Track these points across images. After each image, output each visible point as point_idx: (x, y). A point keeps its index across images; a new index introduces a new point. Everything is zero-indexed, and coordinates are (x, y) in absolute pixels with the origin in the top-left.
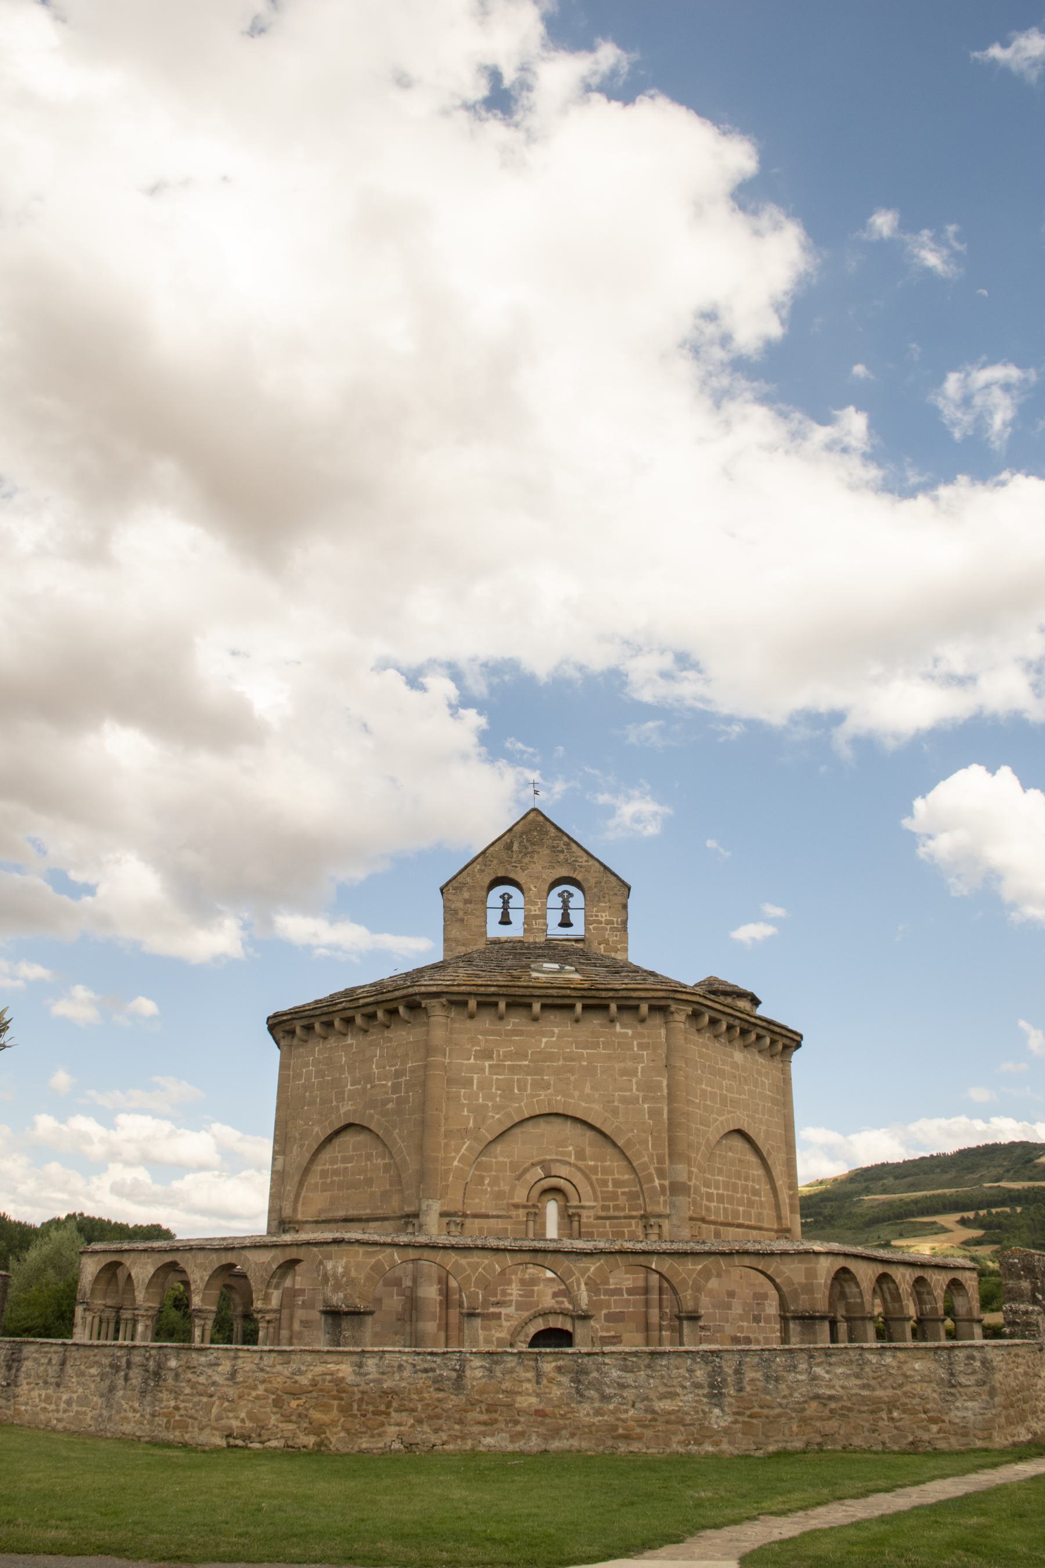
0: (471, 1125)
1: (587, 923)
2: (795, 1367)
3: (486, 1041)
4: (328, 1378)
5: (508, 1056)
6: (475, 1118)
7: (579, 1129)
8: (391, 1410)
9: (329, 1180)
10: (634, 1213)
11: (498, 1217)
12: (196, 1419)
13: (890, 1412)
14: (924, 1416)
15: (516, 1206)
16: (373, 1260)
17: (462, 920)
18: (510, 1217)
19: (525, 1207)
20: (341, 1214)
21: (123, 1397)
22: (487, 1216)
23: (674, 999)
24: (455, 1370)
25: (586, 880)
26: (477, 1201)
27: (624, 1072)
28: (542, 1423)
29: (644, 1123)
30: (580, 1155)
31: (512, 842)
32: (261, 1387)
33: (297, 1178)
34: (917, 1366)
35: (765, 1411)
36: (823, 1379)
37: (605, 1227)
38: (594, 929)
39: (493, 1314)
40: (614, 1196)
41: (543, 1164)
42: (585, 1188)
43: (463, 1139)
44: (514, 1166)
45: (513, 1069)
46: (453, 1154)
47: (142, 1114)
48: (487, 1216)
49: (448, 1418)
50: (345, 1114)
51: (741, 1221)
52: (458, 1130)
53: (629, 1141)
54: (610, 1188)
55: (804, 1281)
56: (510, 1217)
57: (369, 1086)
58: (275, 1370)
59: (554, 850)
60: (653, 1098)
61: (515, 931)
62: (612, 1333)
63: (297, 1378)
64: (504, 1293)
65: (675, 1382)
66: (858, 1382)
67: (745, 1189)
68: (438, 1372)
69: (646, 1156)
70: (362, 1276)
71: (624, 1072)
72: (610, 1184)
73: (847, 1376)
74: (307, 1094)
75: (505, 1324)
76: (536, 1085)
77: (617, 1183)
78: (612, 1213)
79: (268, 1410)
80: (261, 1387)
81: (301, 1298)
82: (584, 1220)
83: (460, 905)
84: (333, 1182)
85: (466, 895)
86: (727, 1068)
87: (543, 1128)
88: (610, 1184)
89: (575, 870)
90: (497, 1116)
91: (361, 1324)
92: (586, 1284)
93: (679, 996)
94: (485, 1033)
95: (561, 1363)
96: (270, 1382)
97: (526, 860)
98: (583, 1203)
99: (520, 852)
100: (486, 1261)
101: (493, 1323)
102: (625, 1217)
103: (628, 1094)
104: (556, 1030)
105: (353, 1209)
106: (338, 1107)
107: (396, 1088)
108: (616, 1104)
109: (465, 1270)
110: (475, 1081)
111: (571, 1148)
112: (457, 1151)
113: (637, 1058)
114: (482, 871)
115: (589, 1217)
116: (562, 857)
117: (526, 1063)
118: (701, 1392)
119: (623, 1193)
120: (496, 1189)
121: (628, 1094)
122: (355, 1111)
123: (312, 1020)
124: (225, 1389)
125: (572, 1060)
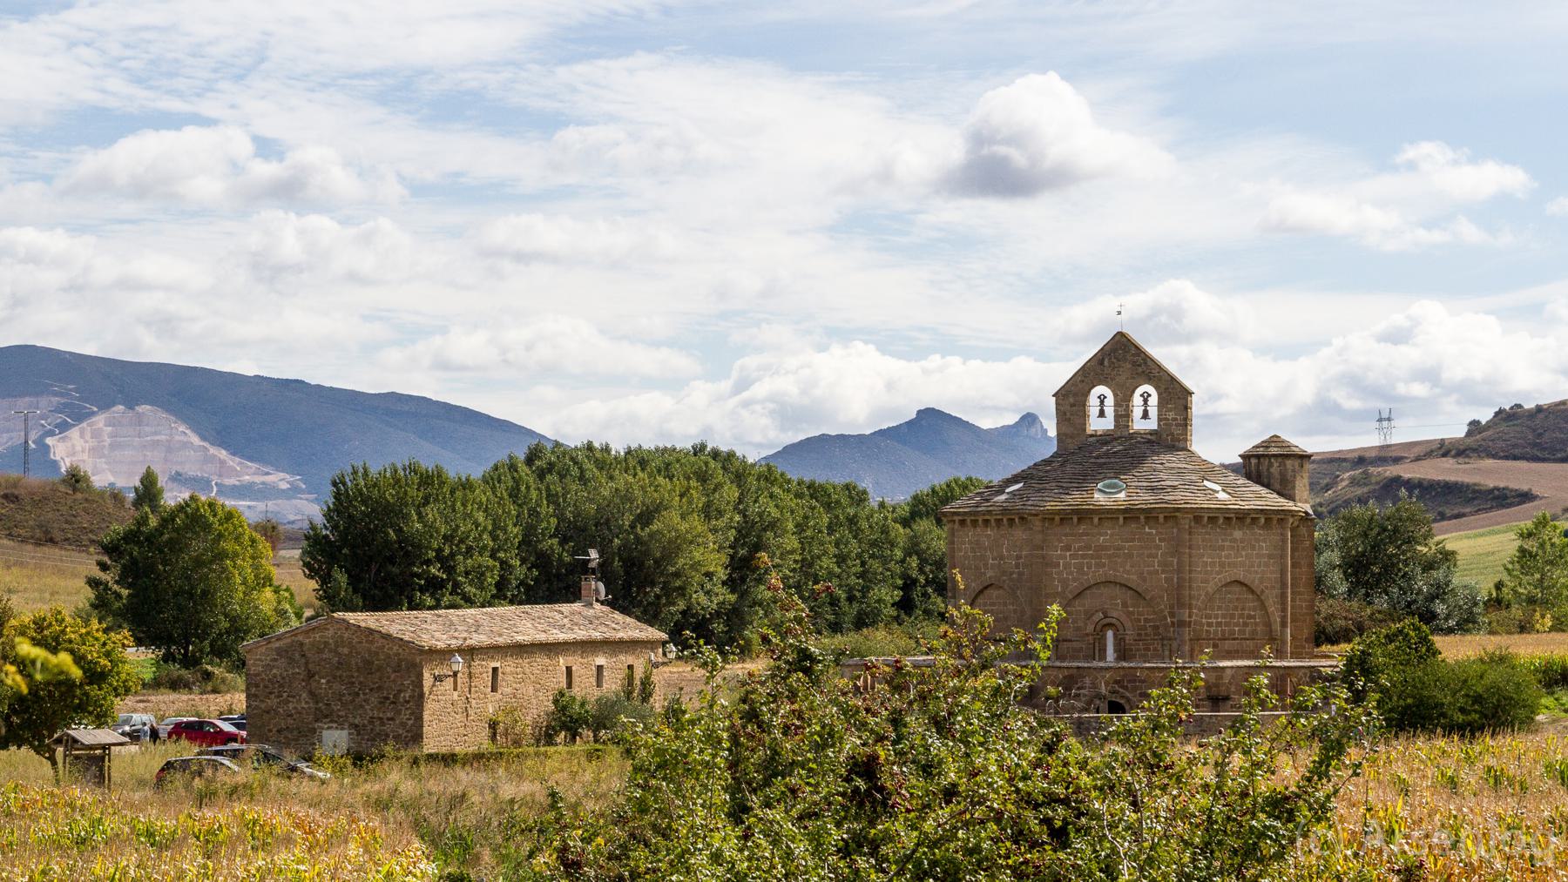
1: (1159, 420)
30: (1125, 605)
42: (1128, 624)
44: (1086, 612)
45: (1083, 557)
59: (1134, 364)
61: (1108, 423)
67: (1241, 616)
76: (1097, 565)
77: (1146, 620)
87: (1104, 590)
107: (1017, 566)
113: (1158, 547)
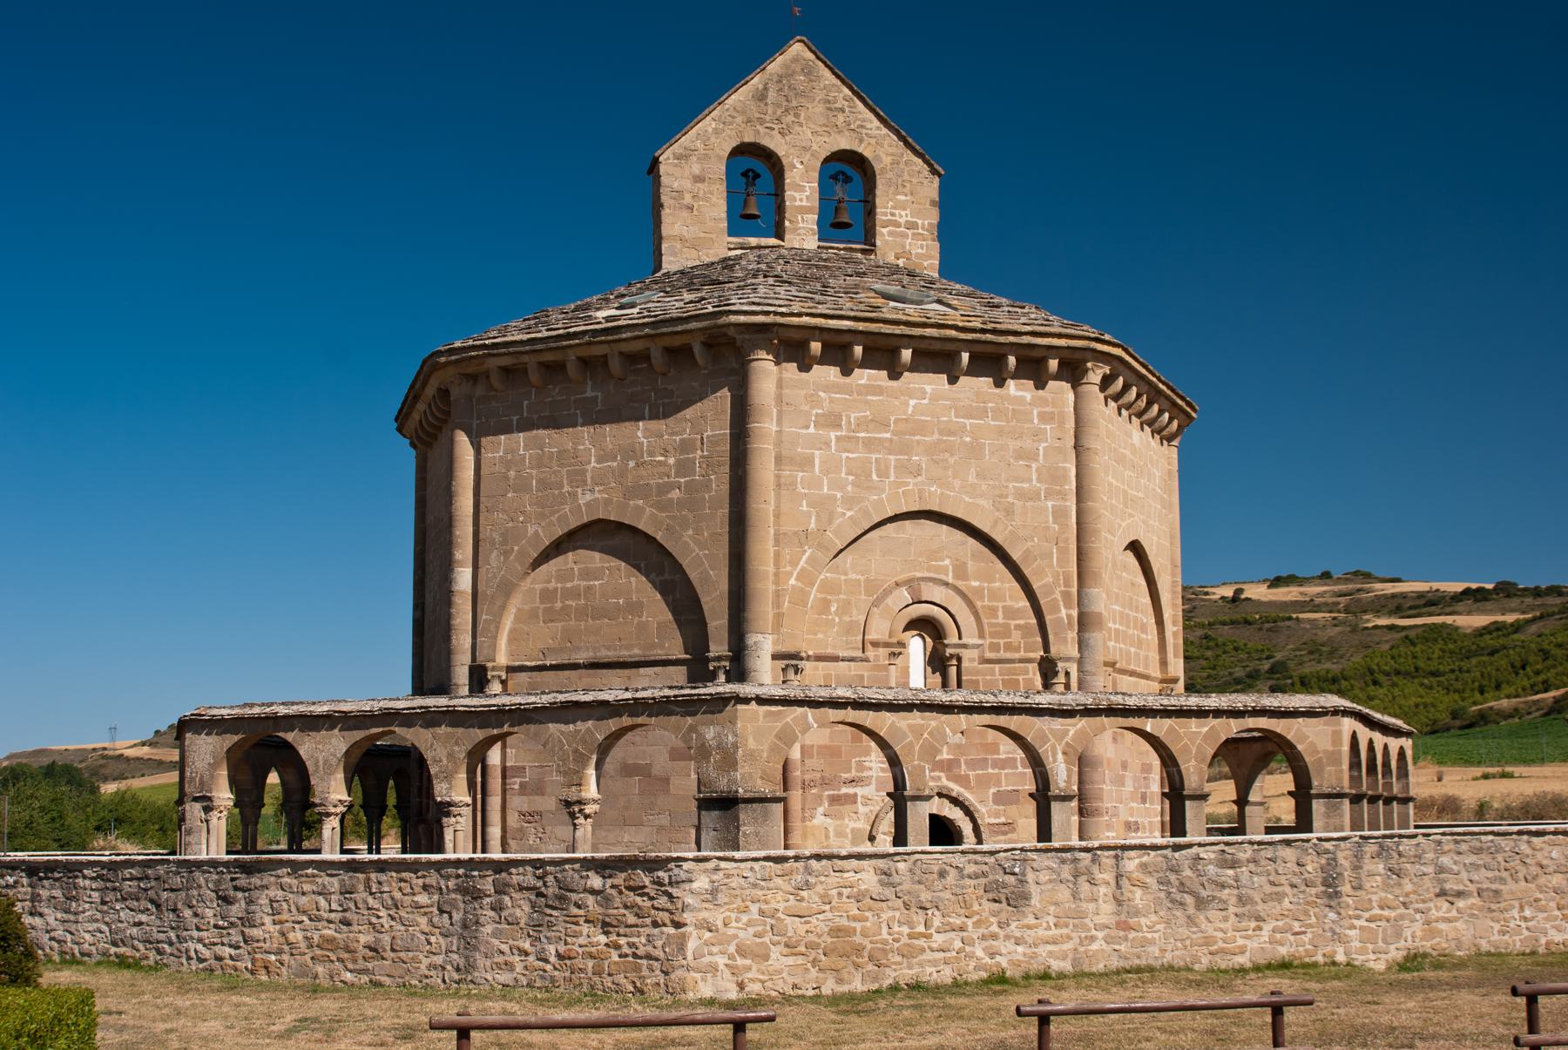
0: (813, 525)
2: (1419, 857)
3: (831, 401)
4: (846, 892)
5: (862, 424)
6: (818, 516)
7: (959, 535)
8: (932, 931)
9: (559, 605)
10: (1031, 655)
11: (851, 660)
12: (657, 959)
13: (1522, 908)
14: (1557, 913)
15: (875, 644)
16: (779, 725)
17: (691, 208)
18: (866, 660)
19: (887, 645)
20: (581, 657)
21: (496, 934)
22: (835, 659)
23: (1094, 350)
24: (1014, 874)
25: (878, 157)
26: (820, 636)
27: (1021, 454)
28: (1126, 939)
29: (1047, 528)
30: (961, 571)
31: (766, 89)
32: (754, 908)
33: (1237, 617)
34: (1554, 855)
35: (1386, 913)
36: (1450, 871)
37: (993, 674)
38: (890, 234)
39: (846, 795)
40: (1005, 632)
41: (910, 583)
43: (801, 546)
44: (870, 586)
45: (869, 444)
46: (788, 568)
47: (417, 502)
48: (835, 659)
49: (1007, 937)
50: (588, 504)
51: (1132, 667)
52: (795, 533)
53: (1027, 553)
54: (1001, 620)
55: (1331, 748)
56: (866, 660)
57: (632, 464)
58: (771, 885)
60: (1059, 492)
62: (1003, 820)
63: (804, 894)
64: (861, 767)
65: (1283, 879)
66: (1490, 874)
68: (991, 878)
69: (1052, 574)
70: (765, 747)
71: (1021, 454)
72: (1000, 614)
73: (1476, 867)
74: (512, 473)
75: (861, 809)
76: (902, 468)
77: (1010, 613)
78: (1003, 655)
79: (766, 939)
80: (754, 908)
81: (518, 780)
82: (965, 664)
83: (687, 184)
84: (565, 608)
85: (696, 169)
86: (1127, 453)
88: (1000, 614)
89: (861, 141)
90: (849, 514)
91: (766, 815)
92: (1064, 753)
93: (1100, 347)
94: (828, 388)
95: (1145, 859)
96: (766, 902)
97: (790, 118)
98: (964, 641)
99: (779, 106)
100: (933, 723)
101: (848, 807)
102: (1021, 661)
103: (1026, 485)
104: (928, 388)
105: (608, 648)
106: (574, 495)
107: (684, 468)
108: (1010, 499)
109: (905, 736)
110: (817, 461)
111: (947, 562)
112: (794, 563)
113: (1037, 435)
114: (716, 132)
115: (972, 660)
116: (841, 118)
117: (888, 435)
118: (1313, 891)
119: (1018, 627)
120: (847, 619)
121: (1026, 485)
122: (607, 502)
123: (526, 358)
124: (704, 914)
125: (951, 433)
